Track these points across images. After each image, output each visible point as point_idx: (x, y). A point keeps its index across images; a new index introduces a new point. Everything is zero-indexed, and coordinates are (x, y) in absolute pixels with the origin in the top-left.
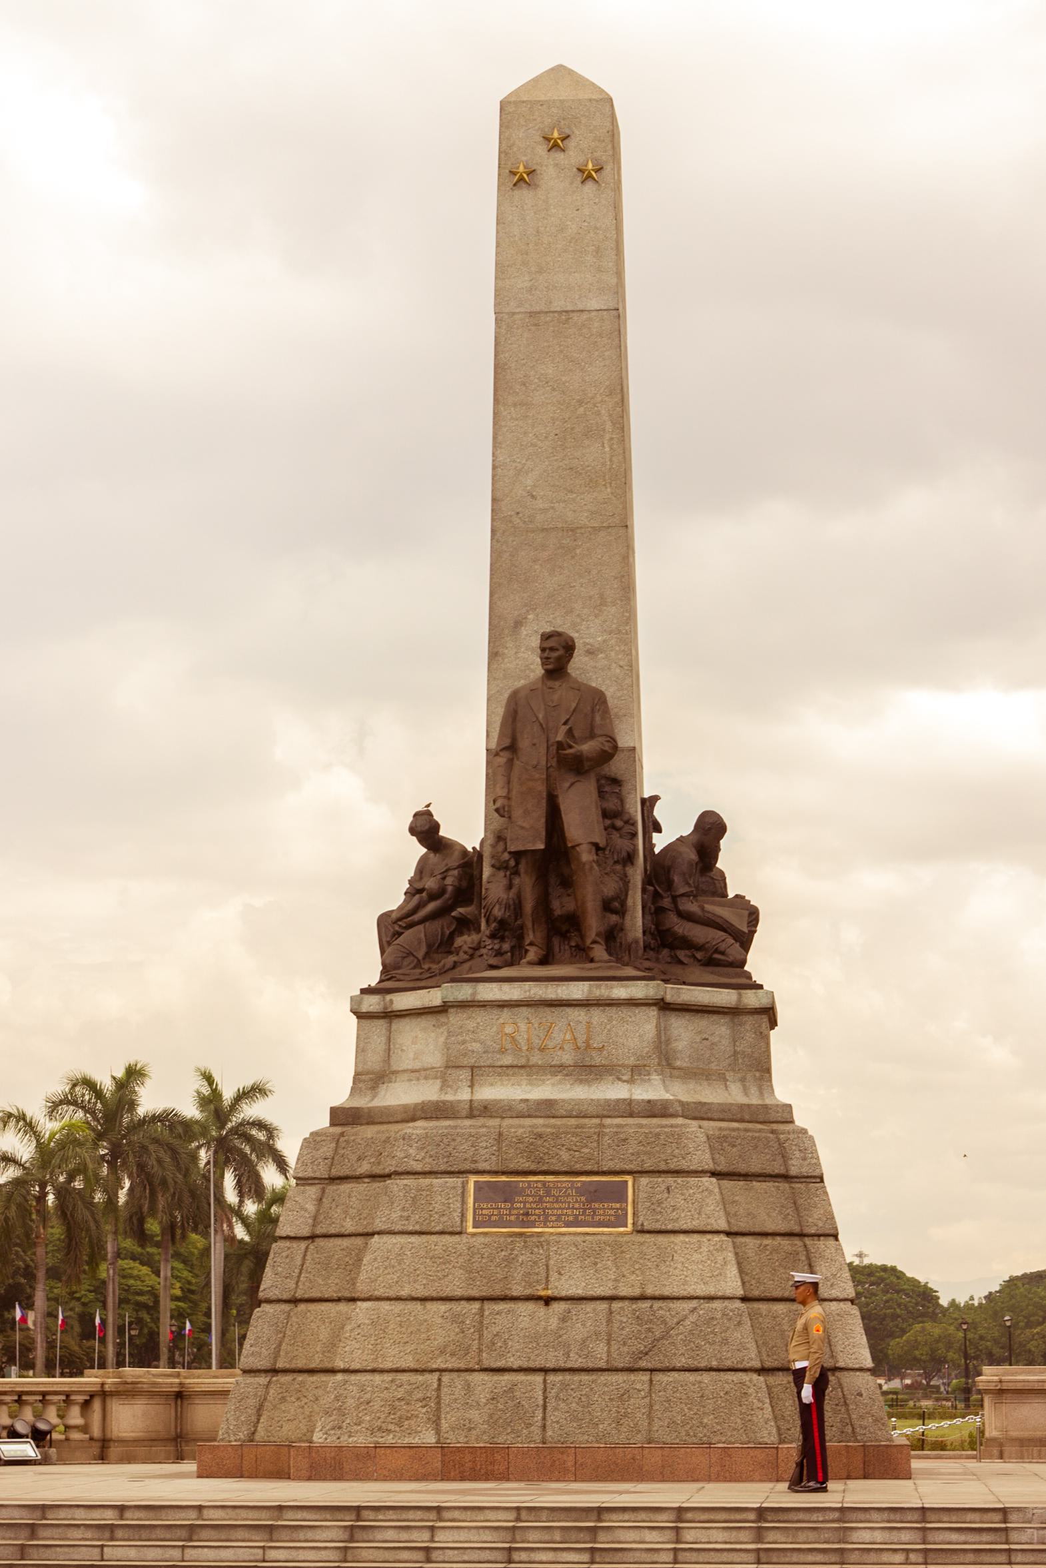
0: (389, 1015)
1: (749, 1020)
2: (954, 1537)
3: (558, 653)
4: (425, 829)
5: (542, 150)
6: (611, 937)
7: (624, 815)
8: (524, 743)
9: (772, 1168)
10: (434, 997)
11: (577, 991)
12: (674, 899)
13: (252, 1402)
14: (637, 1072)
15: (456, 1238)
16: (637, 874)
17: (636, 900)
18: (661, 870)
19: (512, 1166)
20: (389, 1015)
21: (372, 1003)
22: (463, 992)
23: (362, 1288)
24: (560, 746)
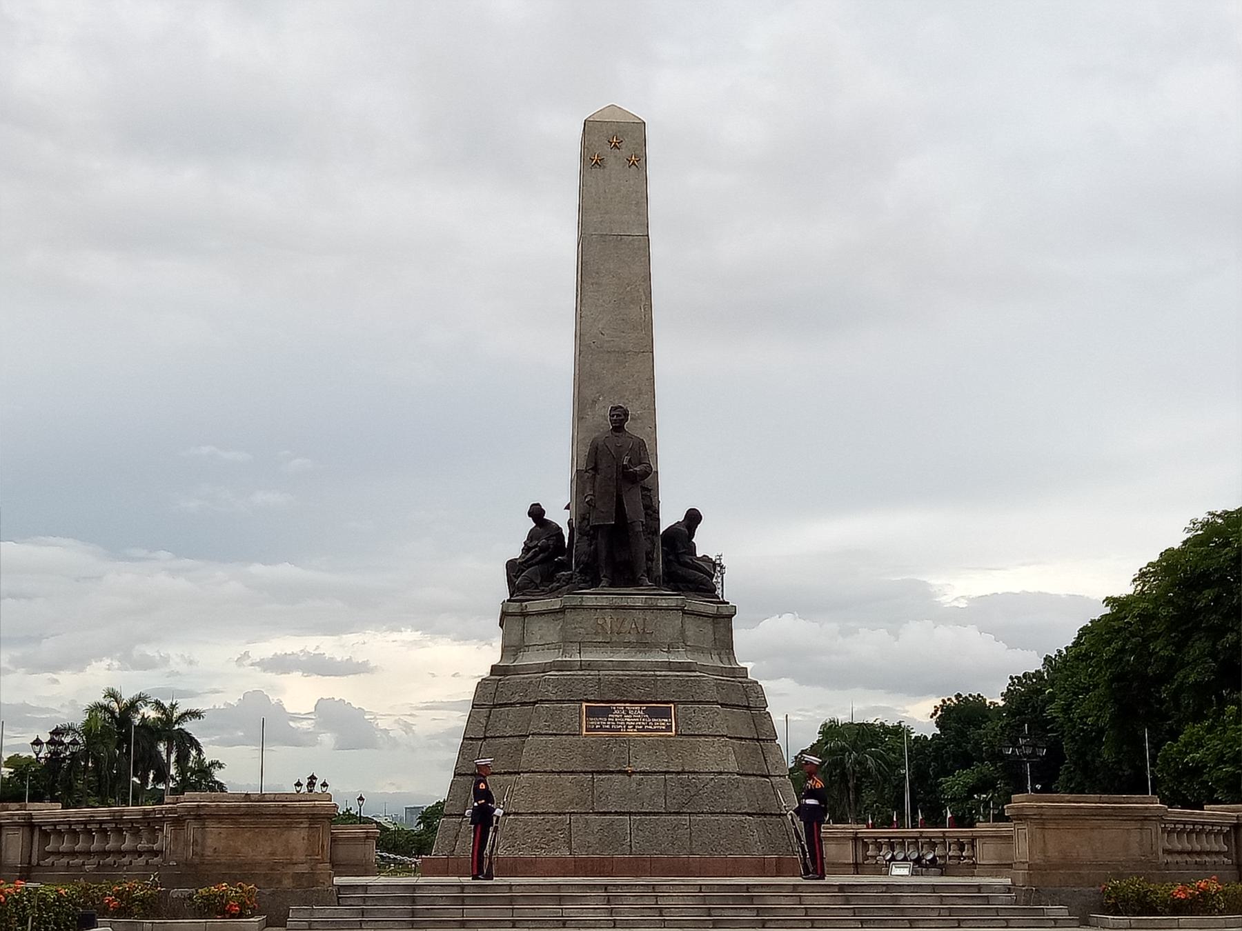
0: (524, 615)
2: (958, 901)
3: (619, 418)
4: (536, 513)
5: (607, 148)
8: (603, 465)
9: (746, 700)
10: (555, 603)
12: (677, 556)
13: (453, 833)
14: (671, 648)
15: (576, 738)
19: (607, 698)
20: (524, 615)
21: (514, 607)
22: (575, 600)
23: (524, 765)
24: (625, 467)
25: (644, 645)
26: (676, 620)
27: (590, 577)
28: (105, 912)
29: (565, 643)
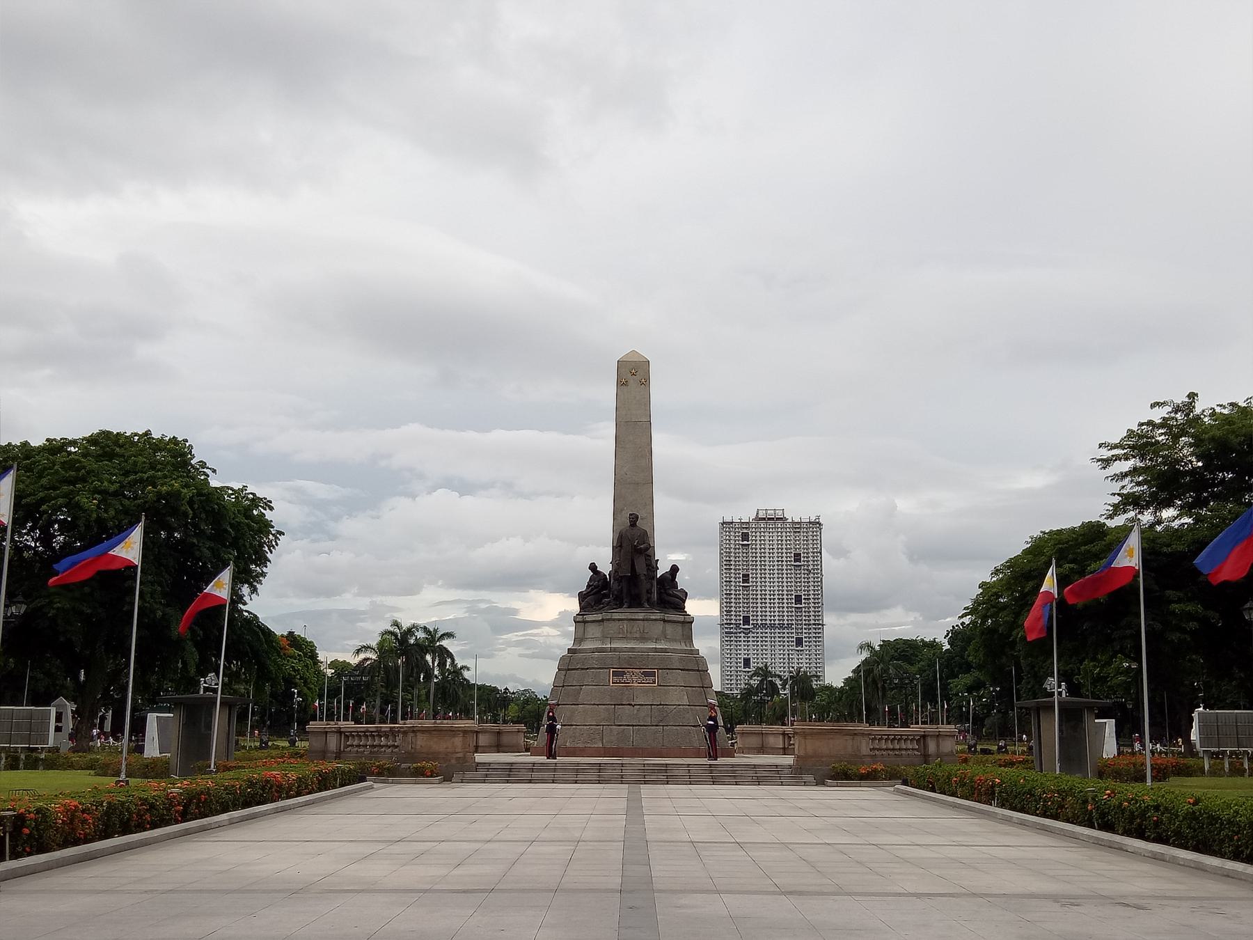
0: (585, 622)
3: (634, 520)
4: (593, 567)
6: (648, 600)
7: (652, 566)
10: (599, 617)
11: (641, 616)
14: (657, 640)
17: (655, 590)
23: (580, 701)
25: (643, 639)
26: (660, 625)
27: (619, 602)
28: (372, 774)
29: (603, 638)
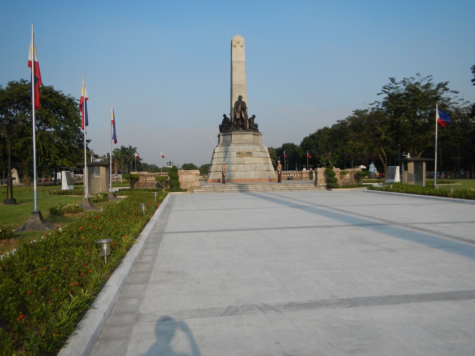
1: (260, 136)
4: (225, 116)
10: (230, 133)
16: (248, 121)
17: (248, 124)
18: (249, 120)
